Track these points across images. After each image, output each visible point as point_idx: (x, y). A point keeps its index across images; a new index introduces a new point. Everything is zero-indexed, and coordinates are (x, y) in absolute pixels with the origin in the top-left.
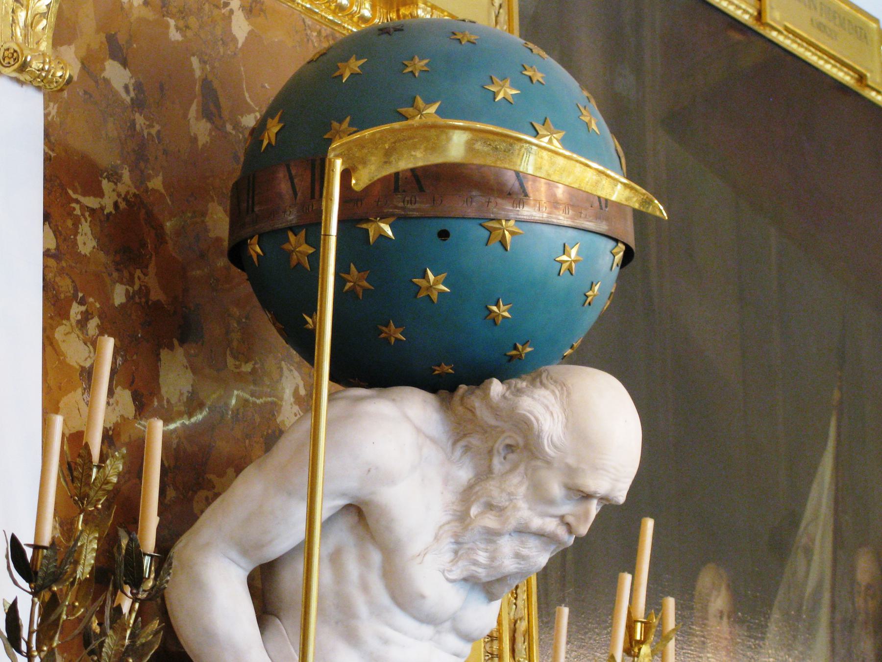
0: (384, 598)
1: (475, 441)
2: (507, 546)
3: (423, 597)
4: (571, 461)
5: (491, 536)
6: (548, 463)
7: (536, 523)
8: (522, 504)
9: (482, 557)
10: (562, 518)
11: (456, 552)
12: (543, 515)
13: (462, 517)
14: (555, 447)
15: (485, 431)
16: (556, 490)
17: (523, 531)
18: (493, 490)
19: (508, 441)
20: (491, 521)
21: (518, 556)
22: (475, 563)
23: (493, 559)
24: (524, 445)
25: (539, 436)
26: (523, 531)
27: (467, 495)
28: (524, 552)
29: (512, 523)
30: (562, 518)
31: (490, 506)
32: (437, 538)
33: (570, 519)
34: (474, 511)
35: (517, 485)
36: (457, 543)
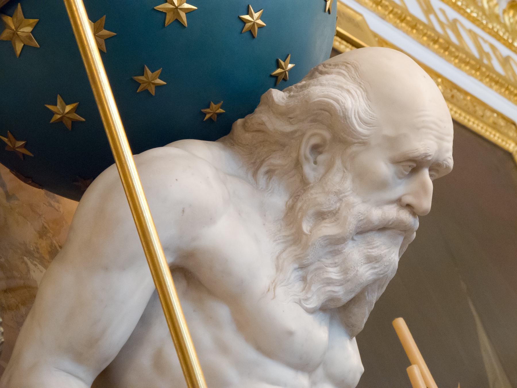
0: (250, 354)
1: (276, 160)
2: (355, 252)
3: (291, 333)
4: (388, 131)
5: (335, 244)
6: (364, 143)
7: (377, 214)
8: (354, 199)
9: (334, 273)
10: (399, 202)
11: (304, 279)
12: (380, 204)
13: (296, 239)
14: (366, 123)
15: (282, 143)
16: (384, 169)
17: (366, 230)
18: (318, 197)
19: (314, 141)
20: (329, 229)
21: (370, 260)
22: (329, 282)
23: (345, 271)
24: (334, 134)
25: (346, 117)
26: (366, 230)
27: (291, 216)
28: (375, 252)
29: (352, 224)
30: (399, 202)
31: (321, 216)
32: (279, 268)
33: (409, 199)
34: (306, 227)
35: (341, 181)
36: (302, 267)
